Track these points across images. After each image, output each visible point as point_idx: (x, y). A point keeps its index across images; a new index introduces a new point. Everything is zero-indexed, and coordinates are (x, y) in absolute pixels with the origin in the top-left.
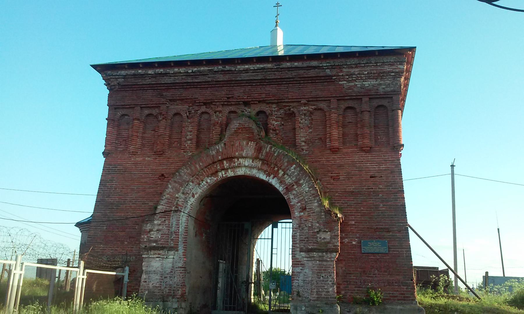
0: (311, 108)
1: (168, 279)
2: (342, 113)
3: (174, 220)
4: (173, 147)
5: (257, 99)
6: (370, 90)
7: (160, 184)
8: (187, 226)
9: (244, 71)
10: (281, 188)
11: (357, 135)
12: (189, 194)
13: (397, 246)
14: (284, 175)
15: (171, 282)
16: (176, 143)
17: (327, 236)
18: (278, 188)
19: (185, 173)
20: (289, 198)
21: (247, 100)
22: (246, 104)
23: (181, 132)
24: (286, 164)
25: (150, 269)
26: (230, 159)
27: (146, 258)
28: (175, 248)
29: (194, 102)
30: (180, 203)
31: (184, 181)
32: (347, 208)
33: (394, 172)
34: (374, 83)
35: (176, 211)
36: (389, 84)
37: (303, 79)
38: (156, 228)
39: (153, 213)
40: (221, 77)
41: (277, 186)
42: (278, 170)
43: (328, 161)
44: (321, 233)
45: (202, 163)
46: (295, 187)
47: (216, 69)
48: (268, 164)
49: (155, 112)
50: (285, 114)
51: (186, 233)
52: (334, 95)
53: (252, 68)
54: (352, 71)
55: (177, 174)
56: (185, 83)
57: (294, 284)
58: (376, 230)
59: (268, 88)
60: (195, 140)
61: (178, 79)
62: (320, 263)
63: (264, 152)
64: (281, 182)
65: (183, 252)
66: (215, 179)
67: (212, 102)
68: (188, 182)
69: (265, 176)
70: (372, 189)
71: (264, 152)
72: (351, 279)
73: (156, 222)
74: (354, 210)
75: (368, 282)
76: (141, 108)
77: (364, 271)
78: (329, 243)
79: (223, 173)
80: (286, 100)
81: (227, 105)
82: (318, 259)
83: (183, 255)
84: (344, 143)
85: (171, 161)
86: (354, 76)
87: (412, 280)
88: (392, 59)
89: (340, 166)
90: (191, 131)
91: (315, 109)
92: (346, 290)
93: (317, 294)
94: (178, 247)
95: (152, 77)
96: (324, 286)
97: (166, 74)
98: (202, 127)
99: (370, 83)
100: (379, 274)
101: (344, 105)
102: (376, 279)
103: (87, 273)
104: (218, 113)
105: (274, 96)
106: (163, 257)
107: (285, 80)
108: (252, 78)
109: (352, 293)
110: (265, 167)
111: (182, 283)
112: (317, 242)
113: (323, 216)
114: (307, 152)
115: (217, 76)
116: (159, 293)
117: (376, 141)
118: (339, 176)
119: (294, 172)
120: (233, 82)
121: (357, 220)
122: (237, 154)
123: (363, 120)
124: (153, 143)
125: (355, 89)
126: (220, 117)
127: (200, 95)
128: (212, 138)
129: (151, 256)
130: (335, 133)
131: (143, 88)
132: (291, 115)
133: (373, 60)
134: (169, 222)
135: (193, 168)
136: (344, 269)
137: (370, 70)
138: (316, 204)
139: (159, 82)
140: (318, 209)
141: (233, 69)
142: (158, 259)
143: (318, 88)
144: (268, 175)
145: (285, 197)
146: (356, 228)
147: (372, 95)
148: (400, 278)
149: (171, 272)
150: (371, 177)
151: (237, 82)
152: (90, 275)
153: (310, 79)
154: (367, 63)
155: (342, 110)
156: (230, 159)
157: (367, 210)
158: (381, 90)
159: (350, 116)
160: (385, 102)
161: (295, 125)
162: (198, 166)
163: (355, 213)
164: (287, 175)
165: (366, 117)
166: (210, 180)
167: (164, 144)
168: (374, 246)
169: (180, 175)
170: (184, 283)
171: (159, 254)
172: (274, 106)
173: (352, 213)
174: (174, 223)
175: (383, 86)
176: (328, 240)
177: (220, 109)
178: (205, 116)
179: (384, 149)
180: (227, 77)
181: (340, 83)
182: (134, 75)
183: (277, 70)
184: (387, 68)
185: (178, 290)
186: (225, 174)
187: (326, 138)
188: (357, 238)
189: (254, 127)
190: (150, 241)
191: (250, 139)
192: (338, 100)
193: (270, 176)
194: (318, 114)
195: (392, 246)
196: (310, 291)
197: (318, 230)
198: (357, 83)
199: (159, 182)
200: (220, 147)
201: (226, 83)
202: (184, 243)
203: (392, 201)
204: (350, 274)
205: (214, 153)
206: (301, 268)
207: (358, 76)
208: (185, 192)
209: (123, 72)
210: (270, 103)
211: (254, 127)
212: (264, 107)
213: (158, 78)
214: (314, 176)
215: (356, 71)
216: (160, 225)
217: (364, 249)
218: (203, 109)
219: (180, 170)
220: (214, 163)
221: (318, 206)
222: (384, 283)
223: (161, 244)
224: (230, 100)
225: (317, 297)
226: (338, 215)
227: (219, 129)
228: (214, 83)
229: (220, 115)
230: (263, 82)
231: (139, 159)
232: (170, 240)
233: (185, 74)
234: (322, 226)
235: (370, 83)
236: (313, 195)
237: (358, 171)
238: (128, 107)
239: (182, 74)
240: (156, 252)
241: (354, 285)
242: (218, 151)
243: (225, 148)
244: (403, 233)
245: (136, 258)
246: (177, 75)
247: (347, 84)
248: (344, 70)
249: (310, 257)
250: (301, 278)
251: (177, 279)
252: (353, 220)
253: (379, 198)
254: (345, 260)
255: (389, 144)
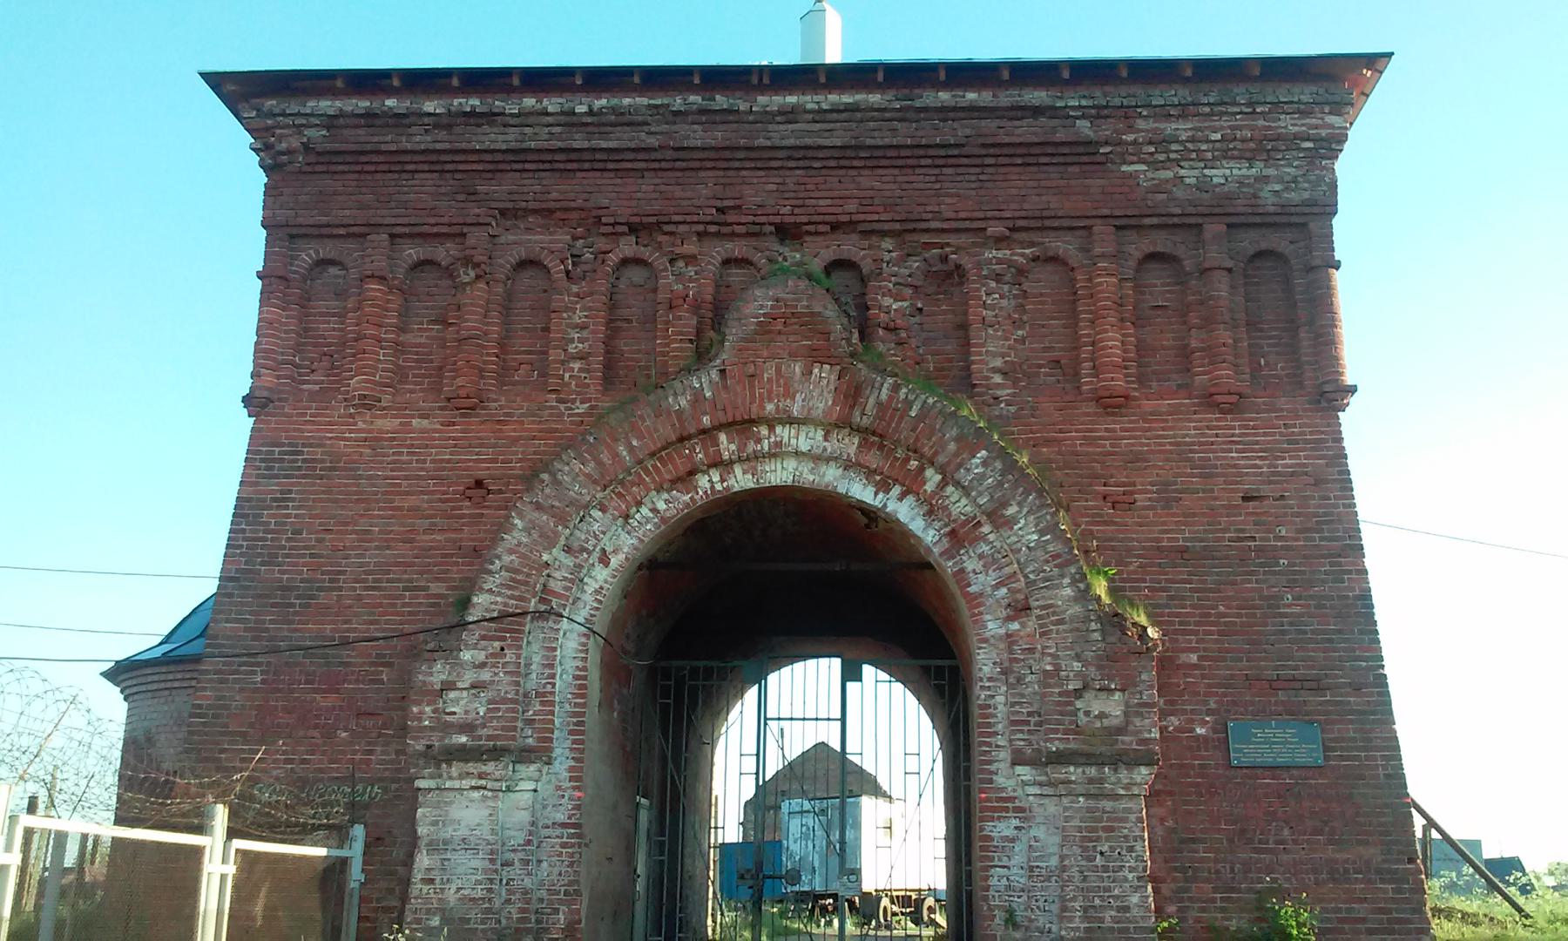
0: (1021, 255)
1: (516, 871)
2: (1130, 273)
3: (535, 647)
4: (514, 384)
5: (828, 218)
6: (1229, 197)
7: (471, 516)
8: (585, 669)
9: (780, 113)
10: (932, 532)
11: (1185, 353)
12: (590, 553)
13: (1354, 740)
14: (942, 485)
15: (528, 882)
16: (524, 369)
17: (1112, 707)
18: (919, 533)
19: (573, 474)
20: (962, 570)
21: (792, 219)
22: (787, 233)
23: (547, 329)
24: (952, 446)
25: (448, 832)
26: (743, 426)
27: (430, 790)
28: (539, 753)
29: (594, 221)
30: (556, 586)
31: (571, 503)
32: (1167, 606)
33: (1328, 482)
34: (1244, 172)
35: (540, 616)
36: (1295, 180)
37: (992, 151)
38: (469, 677)
39: (451, 624)
40: (696, 136)
41: (917, 525)
42: (921, 469)
43: (1091, 441)
44: (1088, 695)
45: (640, 437)
46: (986, 529)
47: (678, 102)
48: (881, 447)
49: (444, 252)
50: (928, 274)
51: (582, 696)
52: (1106, 212)
53: (810, 106)
54: (1170, 127)
55: (545, 476)
56: (561, 150)
57: (993, 882)
58: (1274, 685)
59: (868, 180)
60: (597, 362)
61: (538, 137)
62: (1092, 803)
63: (872, 401)
64: (930, 513)
65: (571, 769)
66: (687, 498)
67: (658, 223)
68: (586, 507)
69: (871, 490)
70: (1254, 539)
71: (872, 401)
72: (1202, 860)
73: (466, 656)
74: (1193, 615)
75: (1259, 871)
76: (392, 236)
77: (1243, 831)
78: (1121, 730)
79: (716, 478)
80: (934, 225)
81: (718, 234)
82: (1080, 789)
83: (571, 779)
84: (1142, 379)
85: (510, 431)
86: (1174, 147)
87: (1412, 860)
88: (1304, 93)
89: (1137, 458)
90: (583, 327)
91: (1035, 259)
92: (1181, 900)
93: (1085, 918)
94: (551, 750)
95: (436, 126)
96: (1108, 889)
97: (491, 117)
98: (625, 312)
99: (1228, 172)
100: (1295, 842)
101: (1138, 246)
102: (1285, 857)
103: (237, 851)
104: (681, 264)
105: (887, 208)
106: (496, 785)
107: (931, 152)
108: (808, 141)
109: (1203, 910)
110: (873, 459)
111: (570, 883)
112: (1078, 730)
113: (1097, 636)
114: (1012, 409)
115: (682, 129)
116: (483, 922)
117: (1256, 369)
118: (1132, 493)
119: (983, 477)
120: (741, 155)
121: (1205, 650)
122: (770, 407)
123: (1211, 298)
124: (441, 368)
125: (1179, 193)
126: (691, 280)
127: (616, 196)
128: (664, 354)
129: (448, 784)
130: (1113, 341)
131: (398, 163)
132: (949, 277)
133: (1241, 93)
134: (518, 656)
135: (605, 457)
136: (1170, 823)
137: (1232, 128)
138: (1068, 592)
139: (464, 146)
140: (1077, 609)
141: (743, 106)
142: (476, 794)
143: (1048, 183)
144: (883, 487)
145: (949, 566)
146: (1203, 677)
147: (1236, 215)
148: (1373, 853)
149: (529, 842)
150: (1245, 499)
151: (753, 155)
152: (245, 857)
153: (1019, 151)
154: (1223, 103)
155: (1132, 263)
156: (743, 426)
157: (1239, 616)
158: (1268, 196)
159: (1159, 283)
160: (1278, 241)
161: (966, 313)
162: (622, 450)
163: (1198, 624)
164: (957, 484)
165: (1221, 288)
166: (660, 508)
167: (482, 370)
168: (1271, 743)
169: (556, 483)
170: (577, 882)
171: (480, 776)
172: (887, 244)
173: (1188, 623)
174: (536, 659)
175: (1274, 183)
176: (1115, 722)
177: (690, 248)
178: (636, 275)
179: (1283, 402)
180: (718, 136)
181: (1124, 168)
182: (369, 115)
183: (903, 115)
184: (1288, 124)
185: (557, 911)
186: (722, 481)
187: (1077, 362)
188: (1210, 712)
189: (828, 313)
190: (447, 728)
191: (817, 356)
192: (1118, 228)
193: (887, 491)
194: (1045, 274)
195: (1335, 740)
196: (1055, 908)
197: (1079, 685)
198: (1182, 172)
199: (467, 509)
200: (705, 382)
201: (712, 154)
202: (571, 733)
203: (1324, 582)
204: (1193, 841)
205: (683, 403)
206: (1016, 822)
207: (1189, 145)
208: (576, 545)
209: (326, 105)
210: (872, 232)
211: (831, 312)
212: (849, 247)
213: (457, 130)
214: (1051, 489)
215: (1182, 128)
216: (483, 665)
217: (1236, 751)
218: (627, 247)
219: (557, 465)
220: (682, 439)
221: (1076, 599)
222: (1315, 871)
223: (489, 738)
224: (730, 218)
225: (1088, 930)
226: (1150, 631)
227: (687, 321)
228: (670, 154)
229: (691, 271)
230: (848, 157)
231: (387, 424)
232: (520, 724)
233: (562, 119)
234: (1092, 672)
235: (1228, 172)
236: (1055, 557)
237: (1201, 475)
238: (342, 231)
239: (550, 119)
240: (471, 767)
241: (1208, 881)
242: (698, 397)
243: (725, 387)
244: (1372, 694)
245: (385, 790)
246: (531, 120)
247: (1150, 175)
248: (1141, 124)
249: (1050, 784)
250: (1018, 859)
251: (550, 870)
252: (1192, 650)
253: (1279, 573)
254: (1171, 793)
255: (1301, 384)
